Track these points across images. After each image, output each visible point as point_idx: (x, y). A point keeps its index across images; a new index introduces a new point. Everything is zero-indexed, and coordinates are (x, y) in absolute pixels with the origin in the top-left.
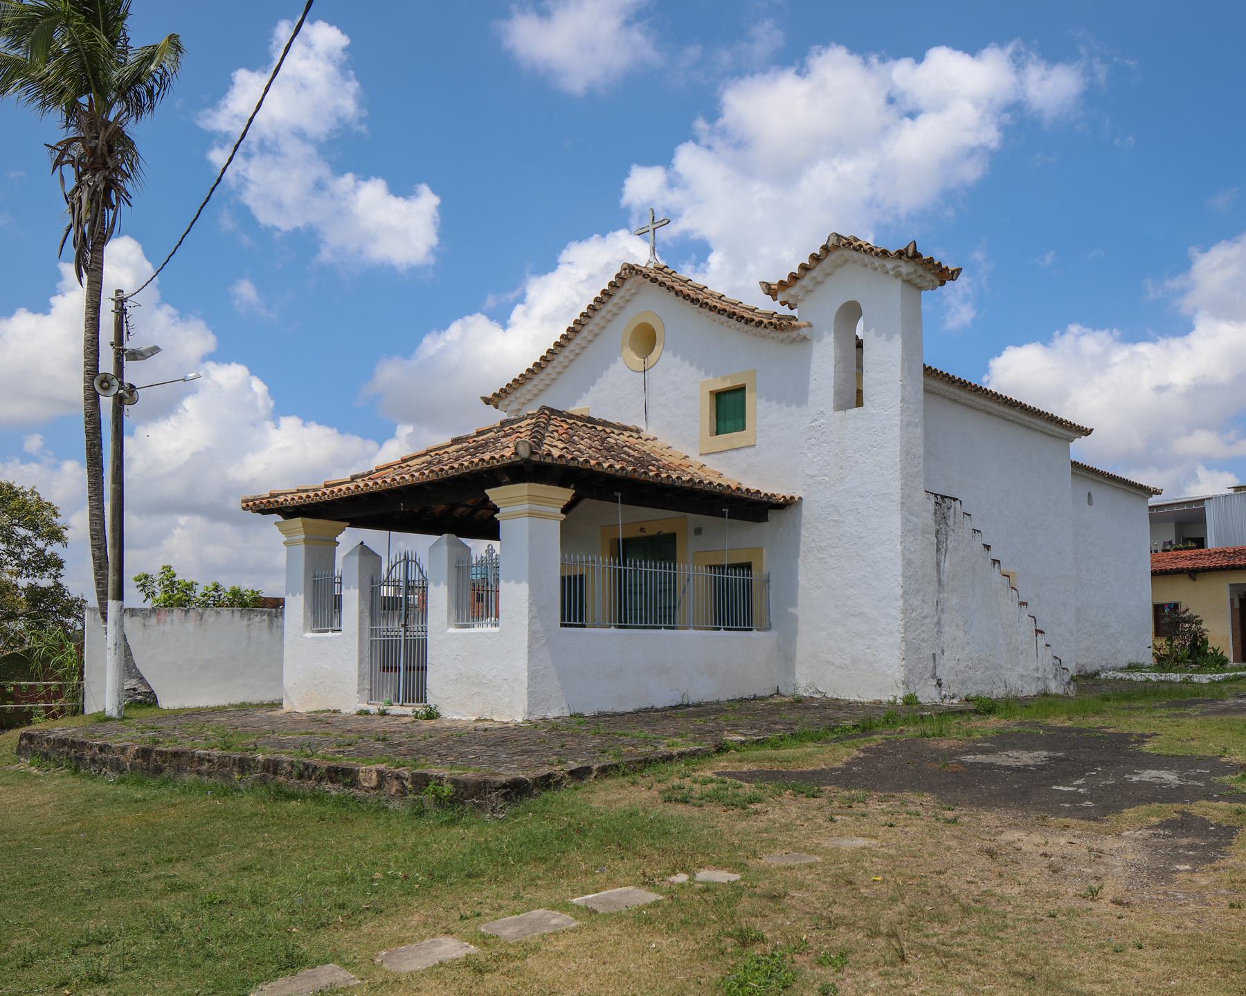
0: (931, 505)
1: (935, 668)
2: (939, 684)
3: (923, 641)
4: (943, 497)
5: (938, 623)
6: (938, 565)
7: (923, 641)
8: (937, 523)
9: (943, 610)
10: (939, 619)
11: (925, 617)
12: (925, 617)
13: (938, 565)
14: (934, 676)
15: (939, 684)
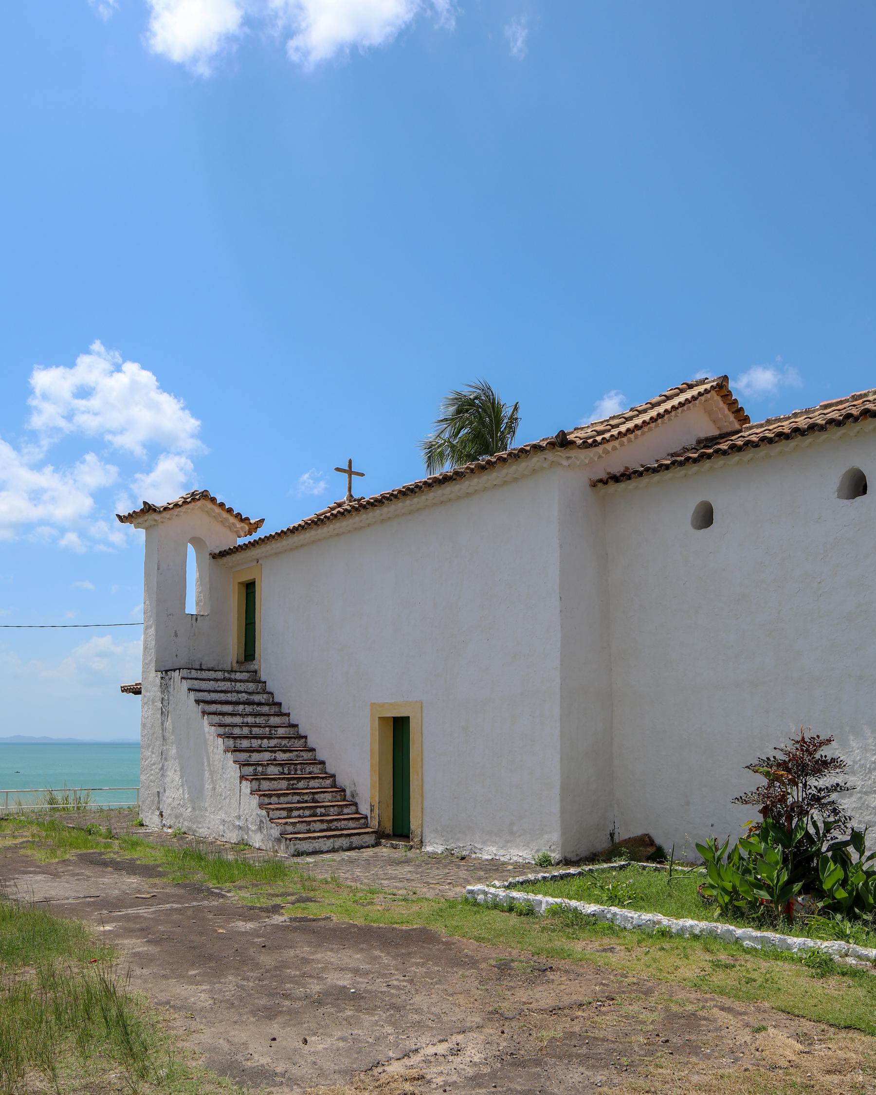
0: (158, 680)
1: (159, 802)
2: (161, 815)
3: (151, 781)
4: (166, 671)
5: (162, 768)
6: (162, 724)
7: (151, 781)
8: (163, 692)
9: (166, 759)
10: (163, 765)
11: (154, 764)
12: (154, 764)
13: (162, 724)
14: (158, 809)
15: (161, 815)
